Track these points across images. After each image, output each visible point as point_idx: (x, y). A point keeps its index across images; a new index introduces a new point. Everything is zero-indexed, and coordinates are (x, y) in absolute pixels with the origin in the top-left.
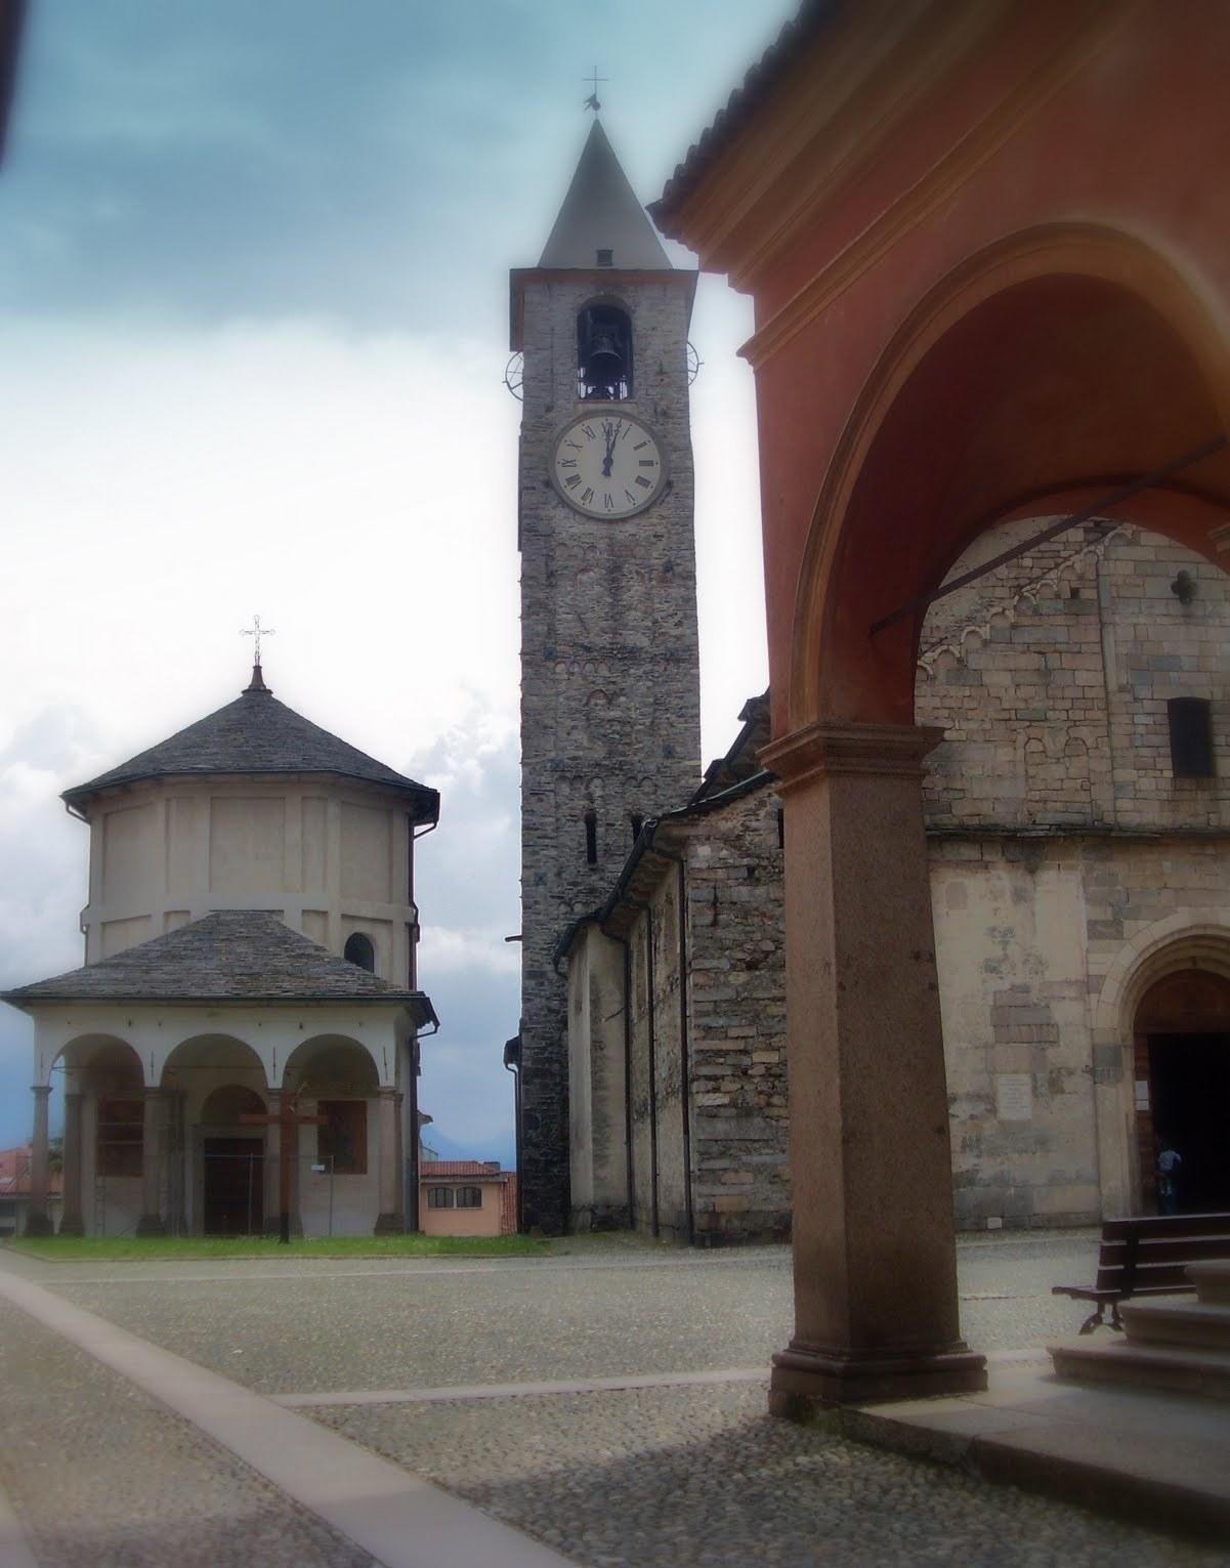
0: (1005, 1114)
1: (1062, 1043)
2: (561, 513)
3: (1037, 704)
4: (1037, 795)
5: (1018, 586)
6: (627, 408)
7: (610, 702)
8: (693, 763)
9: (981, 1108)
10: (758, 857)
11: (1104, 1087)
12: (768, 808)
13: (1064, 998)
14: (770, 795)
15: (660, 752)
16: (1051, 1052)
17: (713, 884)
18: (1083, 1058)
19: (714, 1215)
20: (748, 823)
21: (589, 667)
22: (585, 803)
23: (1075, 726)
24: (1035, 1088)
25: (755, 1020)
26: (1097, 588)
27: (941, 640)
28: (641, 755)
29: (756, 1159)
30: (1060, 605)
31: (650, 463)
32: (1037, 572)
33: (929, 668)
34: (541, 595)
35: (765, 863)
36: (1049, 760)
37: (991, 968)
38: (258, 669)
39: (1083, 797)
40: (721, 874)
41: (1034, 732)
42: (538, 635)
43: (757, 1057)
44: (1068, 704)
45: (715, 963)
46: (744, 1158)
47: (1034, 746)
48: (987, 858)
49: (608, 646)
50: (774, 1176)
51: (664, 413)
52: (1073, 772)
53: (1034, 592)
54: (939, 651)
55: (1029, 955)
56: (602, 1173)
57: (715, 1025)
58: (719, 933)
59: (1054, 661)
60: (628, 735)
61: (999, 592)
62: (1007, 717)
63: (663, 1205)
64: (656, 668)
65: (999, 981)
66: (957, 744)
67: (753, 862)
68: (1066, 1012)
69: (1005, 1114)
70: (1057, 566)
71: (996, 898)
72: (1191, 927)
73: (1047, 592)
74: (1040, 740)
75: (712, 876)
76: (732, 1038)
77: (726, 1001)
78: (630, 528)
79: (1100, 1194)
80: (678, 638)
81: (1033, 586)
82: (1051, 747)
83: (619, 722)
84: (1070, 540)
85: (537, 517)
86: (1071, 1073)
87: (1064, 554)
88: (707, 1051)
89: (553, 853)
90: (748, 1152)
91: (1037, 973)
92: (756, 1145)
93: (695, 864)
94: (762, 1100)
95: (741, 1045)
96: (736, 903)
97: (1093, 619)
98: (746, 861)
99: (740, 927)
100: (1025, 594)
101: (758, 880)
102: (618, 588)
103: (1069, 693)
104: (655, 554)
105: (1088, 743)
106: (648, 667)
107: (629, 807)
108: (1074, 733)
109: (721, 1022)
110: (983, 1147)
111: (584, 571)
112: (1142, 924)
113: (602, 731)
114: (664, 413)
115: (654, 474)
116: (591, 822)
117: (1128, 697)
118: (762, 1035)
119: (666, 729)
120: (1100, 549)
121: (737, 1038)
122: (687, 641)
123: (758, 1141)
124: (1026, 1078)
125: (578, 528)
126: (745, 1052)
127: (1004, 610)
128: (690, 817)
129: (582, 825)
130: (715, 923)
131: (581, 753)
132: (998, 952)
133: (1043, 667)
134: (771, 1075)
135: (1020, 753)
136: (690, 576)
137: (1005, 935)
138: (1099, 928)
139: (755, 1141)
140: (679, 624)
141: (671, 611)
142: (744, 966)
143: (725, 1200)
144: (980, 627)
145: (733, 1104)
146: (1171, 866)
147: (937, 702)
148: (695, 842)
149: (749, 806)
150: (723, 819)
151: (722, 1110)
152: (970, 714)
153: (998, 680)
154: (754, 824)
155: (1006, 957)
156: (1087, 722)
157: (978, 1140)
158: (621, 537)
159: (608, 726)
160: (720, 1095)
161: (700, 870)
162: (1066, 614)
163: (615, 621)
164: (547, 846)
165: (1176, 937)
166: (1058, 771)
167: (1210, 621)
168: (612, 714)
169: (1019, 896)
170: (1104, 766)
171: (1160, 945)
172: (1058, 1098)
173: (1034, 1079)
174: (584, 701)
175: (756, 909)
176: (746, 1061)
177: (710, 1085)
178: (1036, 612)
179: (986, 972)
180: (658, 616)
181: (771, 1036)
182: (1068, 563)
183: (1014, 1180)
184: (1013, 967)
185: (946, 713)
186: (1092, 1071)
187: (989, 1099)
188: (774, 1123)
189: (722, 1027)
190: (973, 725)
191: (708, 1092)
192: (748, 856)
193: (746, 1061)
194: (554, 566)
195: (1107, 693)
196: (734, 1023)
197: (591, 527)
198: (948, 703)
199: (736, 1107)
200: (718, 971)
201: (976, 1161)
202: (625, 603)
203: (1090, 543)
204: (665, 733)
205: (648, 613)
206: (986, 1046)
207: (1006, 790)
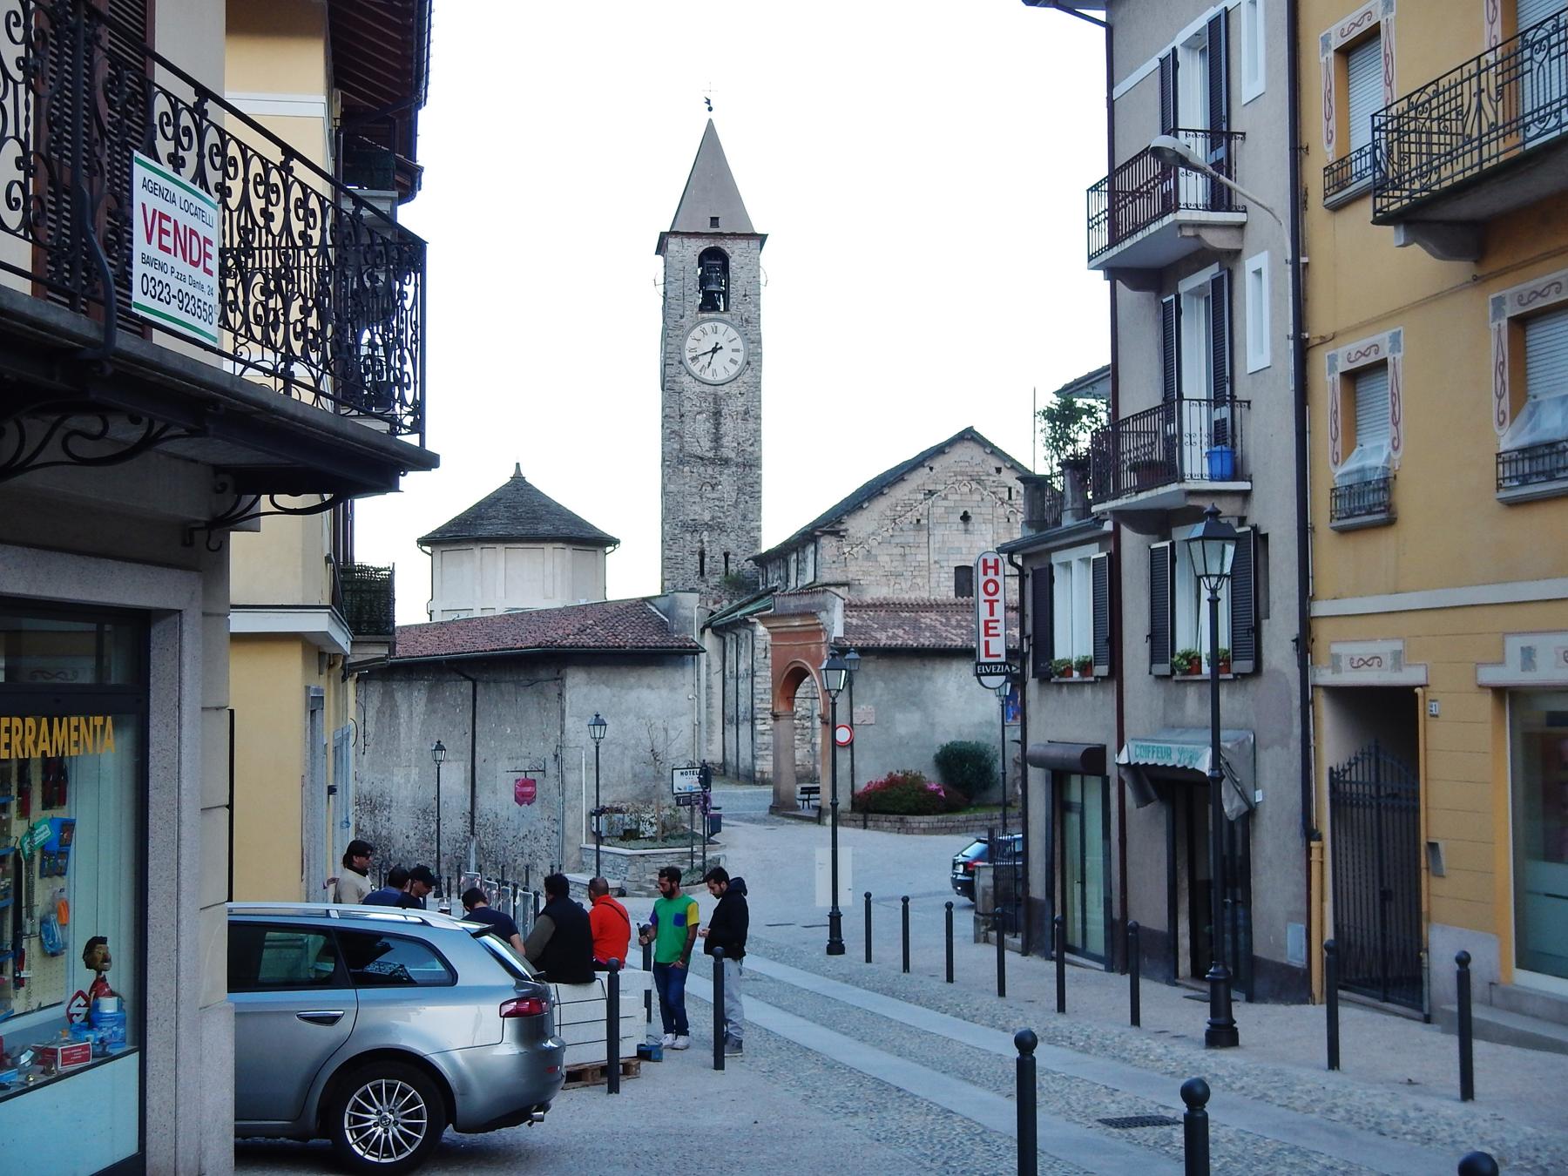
2: (686, 379)
6: (726, 316)
7: (713, 489)
8: (758, 523)
15: (739, 517)
19: (762, 773)
21: (702, 469)
22: (699, 544)
28: (729, 519)
30: (912, 526)
31: (738, 350)
34: (676, 428)
45: (763, 673)
51: (747, 321)
56: (710, 748)
59: (907, 550)
60: (723, 507)
63: (741, 766)
73: (906, 521)
78: (726, 388)
80: (751, 454)
82: (904, 586)
85: (674, 382)
89: (681, 571)
93: (758, 633)
97: (926, 532)
102: (719, 424)
103: (913, 564)
114: (747, 321)
115: (740, 357)
116: (702, 554)
117: (937, 566)
122: (756, 455)
125: (698, 388)
129: (697, 557)
135: (891, 590)
136: (758, 418)
140: (752, 445)
145: (771, 729)
153: (883, 559)
168: (715, 495)
178: (901, 530)
190: (873, 578)
203: (925, 499)
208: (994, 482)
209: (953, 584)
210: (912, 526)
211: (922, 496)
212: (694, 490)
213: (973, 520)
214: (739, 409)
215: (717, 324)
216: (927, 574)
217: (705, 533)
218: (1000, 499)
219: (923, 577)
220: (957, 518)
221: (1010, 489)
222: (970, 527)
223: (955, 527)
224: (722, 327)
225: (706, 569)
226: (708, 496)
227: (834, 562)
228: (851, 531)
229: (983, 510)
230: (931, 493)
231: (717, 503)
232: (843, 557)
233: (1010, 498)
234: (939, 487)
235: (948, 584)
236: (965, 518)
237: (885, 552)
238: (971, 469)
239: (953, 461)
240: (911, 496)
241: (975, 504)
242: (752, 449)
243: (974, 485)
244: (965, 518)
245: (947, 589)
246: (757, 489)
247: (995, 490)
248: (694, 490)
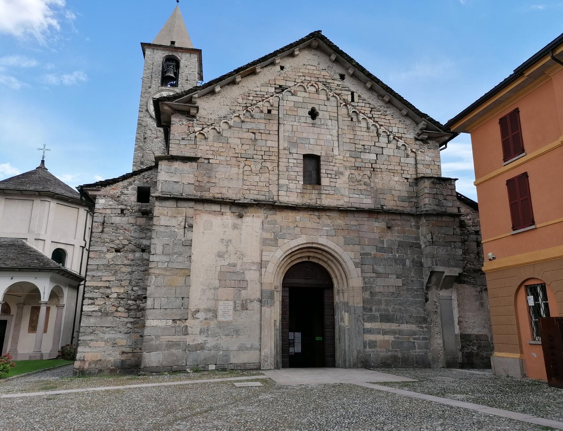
0: (220, 318)
1: (249, 288)
3: (251, 152)
4: (246, 187)
5: (247, 106)
9: (210, 315)
10: (126, 205)
11: (265, 308)
12: (133, 186)
13: (251, 269)
14: (134, 181)
16: (243, 292)
17: (103, 215)
18: (258, 295)
20: (123, 191)
23: (265, 162)
24: (235, 307)
25: (115, 274)
26: (278, 110)
27: (212, 124)
29: (107, 336)
32: (254, 102)
33: (205, 134)
34: (141, 144)
35: (129, 208)
36: (253, 174)
37: (220, 255)
38: (43, 162)
39: (266, 189)
40: (108, 211)
41: (247, 163)
42: (139, 157)
43: (113, 290)
44: (263, 153)
45: (99, 249)
46: (101, 335)
47: (247, 168)
48: (222, 210)
50: (115, 344)
52: (262, 179)
53: (252, 109)
54: (210, 128)
55: (237, 251)
57: (96, 275)
58: (104, 236)
61: (238, 108)
62: (237, 156)
65: (223, 261)
66: (215, 165)
67: (123, 207)
68: (252, 275)
69: (220, 318)
70: (263, 100)
71: (225, 227)
72: (307, 243)
74: (250, 166)
75: (104, 211)
76: (103, 281)
77: (103, 265)
79: (261, 356)
81: (252, 107)
82: (253, 168)
84: (269, 91)
86: (251, 301)
87: (266, 96)
88: (91, 286)
90: (104, 333)
91: (240, 259)
92: (108, 329)
93: (97, 206)
94: (114, 309)
95: (107, 284)
96: (113, 224)
97: (276, 122)
98: (120, 207)
99: (114, 234)
100: (249, 110)
101: (125, 215)
103: (264, 149)
105: (270, 168)
108: (264, 164)
109: (99, 274)
110: (209, 332)
111: (156, 138)
112: (286, 241)
117: (287, 152)
118: (118, 280)
120: (280, 96)
121: (106, 281)
123: (109, 327)
124: (231, 303)
126: (108, 287)
127: (239, 115)
128: (97, 187)
130: (102, 232)
132: (223, 249)
133: (253, 138)
134: (119, 298)
135: (241, 170)
137: (227, 242)
138: (268, 241)
139: (107, 327)
142: (114, 250)
143: (90, 354)
144: (229, 120)
145: (100, 311)
146: (299, 216)
147: (208, 148)
148: (98, 197)
149: (124, 185)
150: (112, 189)
151: (94, 313)
152: (222, 154)
153: (235, 142)
154: (126, 192)
155: (227, 251)
156: (269, 161)
157: (207, 330)
160: (95, 306)
161: (99, 209)
162: (265, 119)
165: (300, 247)
166: (257, 178)
167: (323, 127)
169: (235, 227)
170: (275, 178)
171: (293, 250)
172: (245, 311)
173: (235, 302)
175: (122, 227)
176: (108, 291)
177: (91, 301)
179: (218, 257)
181: (121, 281)
182: (268, 100)
183: (222, 347)
184: (230, 256)
185: (211, 152)
186: (261, 301)
187: (214, 312)
188: (118, 319)
189: (99, 276)
190: (222, 158)
191: (89, 305)
192: (122, 204)
193: (108, 291)
194: (146, 136)
195: (279, 150)
196: (106, 274)
198: (212, 148)
199: (101, 311)
200: (101, 252)
201: (205, 339)
206: (216, 289)
207: (233, 184)
208: (338, 85)
209: (302, 169)
210: (263, 115)
211: (273, 90)
213: (320, 116)
216: (276, 158)
218: (344, 100)
219: (272, 161)
220: (305, 112)
221: (352, 94)
222: (317, 121)
223: (303, 120)
227: (183, 139)
228: (202, 112)
229: (329, 109)
230: (281, 89)
232: (193, 136)
233: (353, 100)
234: (291, 84)
235: (297, 169)
236: (313, 114)
237: (236, 135)
238: (318, 72)
239: (301, 64)
240: (263, 89)
241: (322, 103)
243: (321, 86)
244: (313, 114)
245: (295, 174)
247: (340, 92)
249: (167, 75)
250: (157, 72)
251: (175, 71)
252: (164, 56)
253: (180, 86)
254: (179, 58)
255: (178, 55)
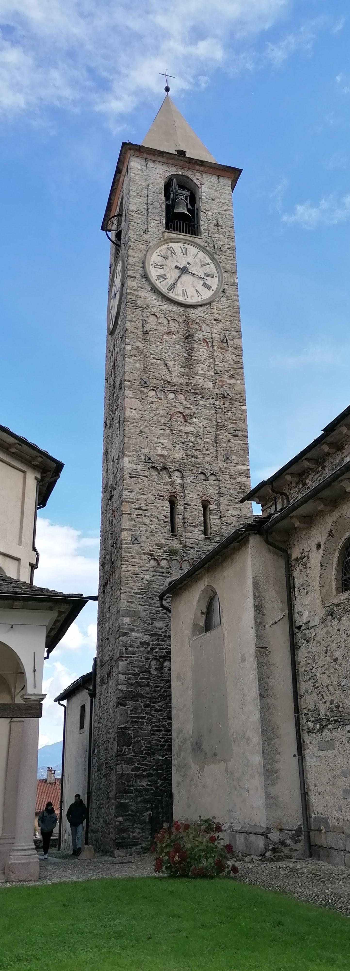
15: (221, 458)
21: (171, 396)
22: (169, 487)
28: (208, 459)
42: (137, 369)
49: (185, 383)
64: (218, 402)
78: (199, 312)
80: (232, 386)
83: (192, 434)
102: (191, 348)
104: (215, 331)
106: (211, 401)
107: (200, 493)
113: (181, 440)
119: (225, 443)
122: (237, 388)
125: (166, 307)
129: (167, 504)
131: (166, 453)
140: (231, 377)
141: (226, 368)
158: (194, 317)
159: (185, 437)
163: (190, 368)
164: (141, 515)
174: (168, 418)
180: (218, 369)
194: (147, 327)
197: (174, 308)
202: (196, 358)
204: (225, 445)
205: (212, 367)
212: (162, 420)
214: (214, 335)
215: (186, 246)
217: (176, 474)
224: (193, 250)
225: (179, 519)
226: (182, 428)
231: (192, 439)
242: (232, 381)
246: (241, 425)
248: (162, 420)
249: (176, 211)
250: (157, 205)
251: (190, 207)
252: (168, 174)
253: (204, 235)
254: (197, 182)
255: (196, 177)
